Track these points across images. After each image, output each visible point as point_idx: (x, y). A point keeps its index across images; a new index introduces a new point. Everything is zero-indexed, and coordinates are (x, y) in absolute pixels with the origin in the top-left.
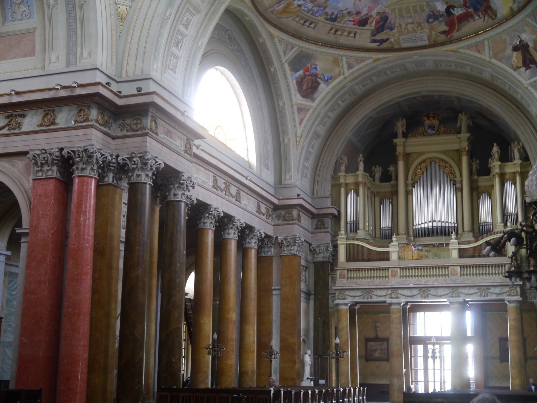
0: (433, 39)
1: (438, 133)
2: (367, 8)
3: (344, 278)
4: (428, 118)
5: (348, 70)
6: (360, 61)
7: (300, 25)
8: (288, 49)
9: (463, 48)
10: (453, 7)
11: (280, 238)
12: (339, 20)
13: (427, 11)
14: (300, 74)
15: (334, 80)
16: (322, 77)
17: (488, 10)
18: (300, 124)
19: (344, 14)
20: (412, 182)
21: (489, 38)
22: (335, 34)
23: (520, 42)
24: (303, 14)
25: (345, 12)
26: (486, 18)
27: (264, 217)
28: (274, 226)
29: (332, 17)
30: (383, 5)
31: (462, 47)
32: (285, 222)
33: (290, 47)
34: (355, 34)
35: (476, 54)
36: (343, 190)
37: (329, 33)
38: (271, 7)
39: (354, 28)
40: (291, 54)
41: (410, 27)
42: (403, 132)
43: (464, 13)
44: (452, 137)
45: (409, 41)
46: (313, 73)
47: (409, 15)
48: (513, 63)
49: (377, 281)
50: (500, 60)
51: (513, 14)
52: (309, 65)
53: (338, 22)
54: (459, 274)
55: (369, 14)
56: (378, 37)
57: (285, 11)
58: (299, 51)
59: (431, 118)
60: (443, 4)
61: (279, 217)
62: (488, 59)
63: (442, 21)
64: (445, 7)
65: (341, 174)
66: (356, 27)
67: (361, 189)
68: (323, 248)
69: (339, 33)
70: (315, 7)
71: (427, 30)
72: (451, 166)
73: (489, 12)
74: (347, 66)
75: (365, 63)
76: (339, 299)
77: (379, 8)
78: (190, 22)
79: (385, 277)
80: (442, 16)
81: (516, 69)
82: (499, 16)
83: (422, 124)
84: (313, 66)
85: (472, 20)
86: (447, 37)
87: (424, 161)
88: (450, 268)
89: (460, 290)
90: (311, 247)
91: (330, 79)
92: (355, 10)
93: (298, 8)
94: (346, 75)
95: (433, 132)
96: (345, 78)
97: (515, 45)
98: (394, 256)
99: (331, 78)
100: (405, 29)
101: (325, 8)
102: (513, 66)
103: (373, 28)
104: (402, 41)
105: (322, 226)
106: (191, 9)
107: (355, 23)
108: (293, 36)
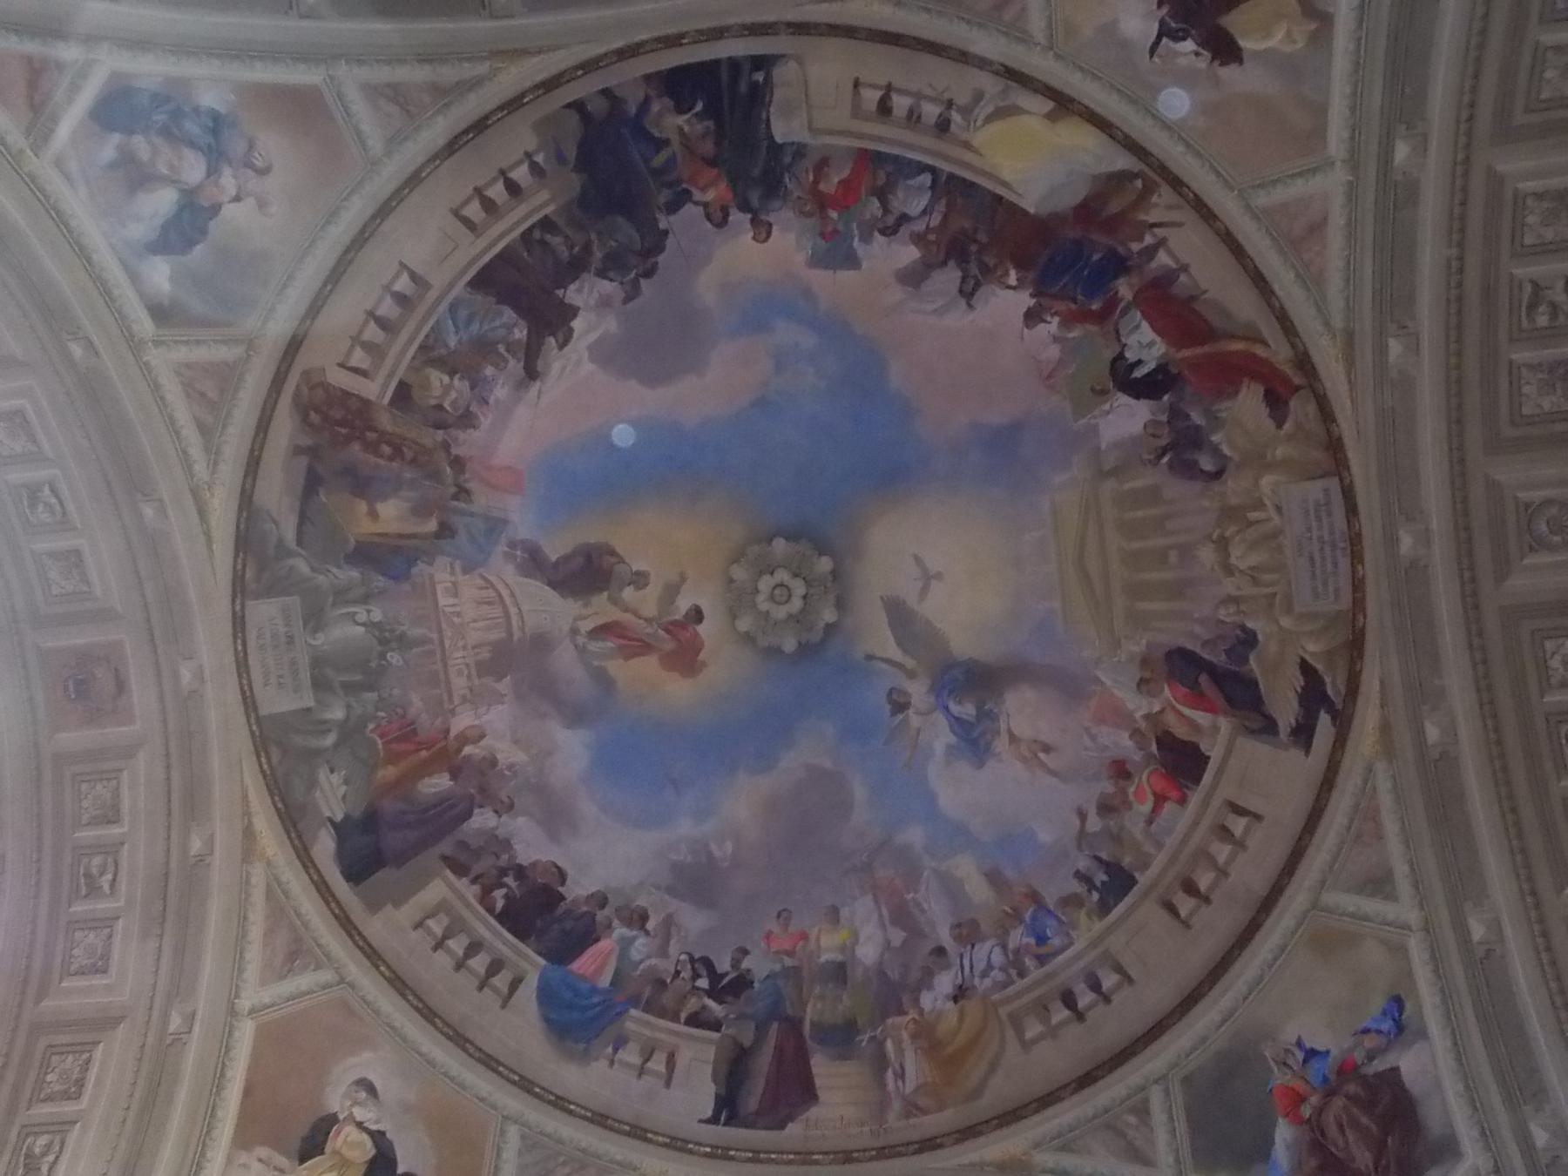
5: (1392, 897)
7: (1076, 1029)
8: (1131, 1133)
9: (1321, 308)
12: (1127, 861)
14: (1288, 1147)
16: (1370, 1042)
17: (1104, 214)
21: (1232, 189)
23: (1177, 37)
24: (1019, 995)
25: (1094, 824)
26: (1152, 218)
29: (1098, 884)
31: (1319, 310)
33: (1132, 1120)
34: (1240, 811)
37: (1186, 924)
39: (1205, 803)
41: (1241, 558)
43: (1146, 316)
45: (1329, 567)
46: (1325, 1079)
47: (1173, 557)
50: (1320, 111)
51: (1063, 105)
52: (1280, 1078)
53: (1145, 866)
55: (1143, 725)
58: (1176, 1088)
60: (1107, 407)
64: (1123, 399)
66: (1195, 798)
69: (1204, 881)
70: (1006, 933)
71: (1267, 481)
74: (1372, 895)
75: (1386, 801)
80: (1176, 413)
84: (1290, 1061)
85: (1183, 278)
86: (1298, 388)
91: (1401, 1009)
93: (972, 1006)
94: (1413, 917)
96: (1428, 928)
97: (1207, 54)
99: (1398, 1001)
100: (1255, 581)
101: (1035, 897)
102: (1314, 38)
103: (1225, 724)
107: (1174, 794)
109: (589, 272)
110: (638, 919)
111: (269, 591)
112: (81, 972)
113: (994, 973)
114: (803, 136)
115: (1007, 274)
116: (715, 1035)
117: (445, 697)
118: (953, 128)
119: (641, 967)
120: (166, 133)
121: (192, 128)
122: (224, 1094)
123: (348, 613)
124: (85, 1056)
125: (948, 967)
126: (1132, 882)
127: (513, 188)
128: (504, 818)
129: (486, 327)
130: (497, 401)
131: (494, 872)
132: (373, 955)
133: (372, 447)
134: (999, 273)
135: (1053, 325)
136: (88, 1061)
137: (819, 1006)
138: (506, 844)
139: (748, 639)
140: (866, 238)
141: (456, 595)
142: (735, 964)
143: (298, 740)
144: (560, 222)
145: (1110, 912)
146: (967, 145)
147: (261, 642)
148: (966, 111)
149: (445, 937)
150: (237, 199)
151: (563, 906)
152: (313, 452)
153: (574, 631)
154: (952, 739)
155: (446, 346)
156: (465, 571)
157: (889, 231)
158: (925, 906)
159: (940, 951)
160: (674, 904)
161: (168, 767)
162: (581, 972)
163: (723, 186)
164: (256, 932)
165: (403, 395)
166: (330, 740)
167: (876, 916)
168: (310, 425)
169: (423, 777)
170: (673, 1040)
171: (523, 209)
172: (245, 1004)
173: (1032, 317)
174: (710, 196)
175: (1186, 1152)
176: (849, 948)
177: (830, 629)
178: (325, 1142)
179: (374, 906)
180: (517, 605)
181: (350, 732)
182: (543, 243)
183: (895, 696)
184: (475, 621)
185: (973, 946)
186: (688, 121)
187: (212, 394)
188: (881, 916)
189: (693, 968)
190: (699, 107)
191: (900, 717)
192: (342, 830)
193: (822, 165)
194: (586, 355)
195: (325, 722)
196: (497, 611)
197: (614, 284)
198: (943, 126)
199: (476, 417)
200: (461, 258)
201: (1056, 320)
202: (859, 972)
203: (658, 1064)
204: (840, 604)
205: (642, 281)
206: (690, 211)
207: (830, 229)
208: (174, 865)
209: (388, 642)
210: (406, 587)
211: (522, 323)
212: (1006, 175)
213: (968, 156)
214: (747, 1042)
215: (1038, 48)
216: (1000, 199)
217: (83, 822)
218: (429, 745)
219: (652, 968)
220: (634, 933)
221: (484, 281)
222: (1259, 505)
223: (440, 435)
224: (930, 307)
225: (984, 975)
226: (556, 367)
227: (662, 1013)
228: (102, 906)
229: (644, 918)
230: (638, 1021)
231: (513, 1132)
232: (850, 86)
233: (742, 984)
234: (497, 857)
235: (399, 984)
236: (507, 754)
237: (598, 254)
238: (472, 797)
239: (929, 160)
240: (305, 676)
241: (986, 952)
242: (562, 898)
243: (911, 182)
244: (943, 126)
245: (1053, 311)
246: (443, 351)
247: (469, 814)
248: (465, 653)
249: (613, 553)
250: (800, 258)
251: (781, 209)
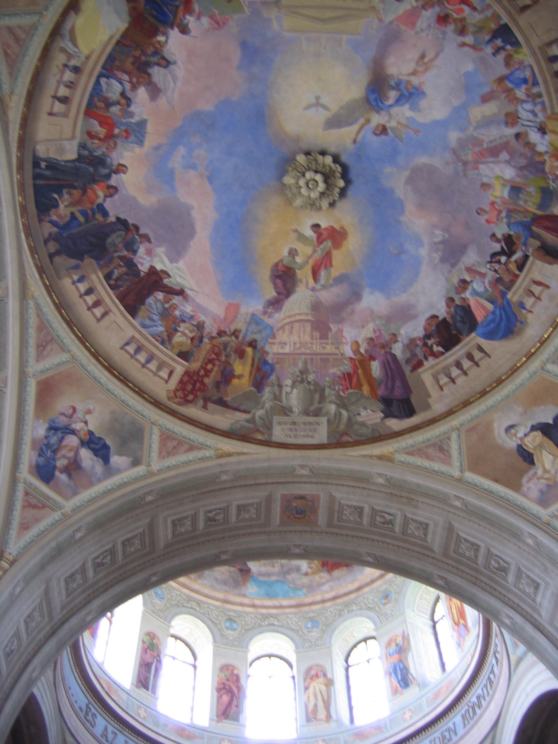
12: (493, 26)
19: (474, 33)
24: (551, 100)
25: (469, 39)
30: (380, 20)
53: (499, 17)
92: (444, 33)
93: (551, 125)
101: (501, 80)
109: (133, 258)
110: (464, 284)
111: (269, 428)
112: (425, 535)
113: (536, 111)
114: (74, 145)
115: (159, 42)
116: (531, 259)
117: (334, 357)
118: (78, 64)
119: (487, 287)
120: (55, 452)
121: (54, 440)
122: (494, 490)
123: (286, 396)
124: (462, 540)
125: (526, 134)
126: (506, 25)
127: (89, 291)
128: (399, 339)
129: (156, 312)
130: (193, 311)
131: (424, 349)
132: (450, 413)
133: (207, 373)
134: (158, 46)
135: (190, 20)
136: (465, 539)
137: (530, 204)
138: (412, 341)
139: (332, 205)
140: (131, 115)
141: (285, 344)
142: (498, 241)
143: (342, 427)
144: (107, 270)
145: (519, 42)
146: (88, 58)
147: (293, 436)
148: (70, 56)
149: (451, 378)
150: (86, 423)
151: (449, 319)
152: (206, 400)
153: (313, 289)
154: (407, 106)
155: (162, 332)
156: (274, 337)
157: (129, 101)
158: (492, 138)
160: (461, 266)
161: (343, 485)
162: (482, 317)
163: (96, 187)
164: (426, 463)
165: (184, 355)
166: (344, 413)
167: (491, 165)
168: (194, 400)
169: (371, 374)
170: (528, 279)
171: (100, 288)
172: (456, 473)
173: (184, 30)
174: (101, 194)
177: (336, 159)
178: (528, 452)
179: (428, 407)
180: (295, 315)
181: (342, 404)
182: (116, 280)
183: (378, 132)
184: (300, 337)
185: (519, 118)
186: (62, 202)
187: (175, 443)
188: (492, 162)
189: (496, 262)
190: (55, 196)
191: (389, 131)
192: (388, 414)
193: (90, 135)
194: (175, 264)
195: (335, 414)
196: (296, 325)
197: (141, 247)
198: (76, 70)
199: (199, 322)
200: (120, 320)
201: (188, 17)
202: (518, 180)
203: (536, 289)
204: (323, 153)
205: (142, 231)
206: (108, 205)
207: (124, 134)
208: (387, 491)
209: (303, 379)
210: (277, 366)
211: (156, 294)
212: (105, 38)
213: (94, 58)
214: (538, 243)
215: (41, 20)
216: (118, 43)
217: (360, 521)
218: (355, 368)
219: (490, 283)
220: (470, 288)
221: (133, 310)
223: (206, 340)
224: (172, 85)
225: (535, 115)
226: (179, 280)
227: (513, 282)
228: (398, 521)
229: (464, 282)
230: (515, 293)
231: (550, 367)
232: (52, 118)
233: (509, 240)
234: (418, 346)
235: (466, 404)
236: (368, 331)
237: (125, 253)
238: (386, 352)
239: (93, 80)
240: (312, 419)
242: (444, 320)
243: (104, 90)
244: (76, 70)
245: (183, 19)
246: (165, 333)
247: (394, 356)
248: (315, 344)
249: (277, 265)
250: (137, 150)
251: (111, 159)
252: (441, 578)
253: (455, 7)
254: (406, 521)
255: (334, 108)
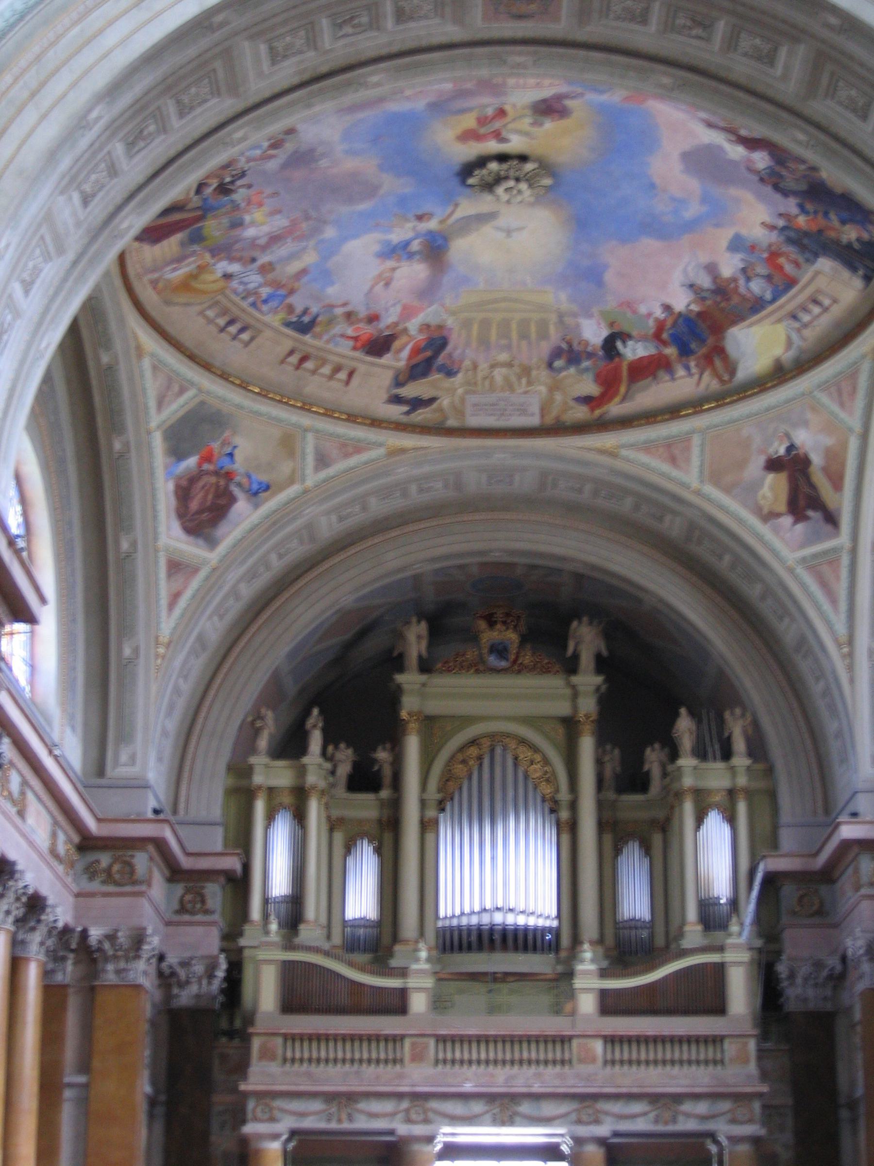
0: (554, 413)
1: (516, 667)
2: (398, 309)
3: (273, 1058)
4: (491, 624)
5: (317, 469)
6: (351, 450)
7: (213, 329)
10: (625, 337)
11: (95, 933)
12: (317, 329)
13: (555, 336)
15: (274, 494)
16: (244, 481)
18: (172, 605)
20: (439, 796)
22: (298, 367)
24: (231, 301)
25: (339, 311)
26: (707, 376)
27: (60, 869)
28: (78, 895)
30: (443, 305)
32: (111, 888)
34: (351, 374)
35: (665, 467)
36: (260, 807)
37: (283, 362)
38: (154, 271)
39: (353, 359)
40: (176, 408)
41: (499, 374)
42: (420, 657)
43: (650, 357)
44: (555, 682)
46: (222, 468)
47: (504, 342)
48: (762, 502)
49: (370, 1071)
50: (727, 490)
52: (216, 446)
54: (600, 1060)
55: (401, 327)
56: (410, 391)
57: (186, 285)
58: (197, 400)
59: (498, 626)
61: (91, 872)
62: (695, 484)
63: (587, 370)
64: (605, 333)
65: (259, 760)
66: (358, 354)
67: (314, 809)
68: (199, 968)
69: (309, 365)
71: (543, 389)
72: (546, 761)
73: (718, 363)
75: (364, 457)
76: (256, 1119)
77: (429, 314)
78: (38, 276)
79: (395, 1061)
80: (590, 355)
81: (769, 516)
82: (742, 374)
83: (474, 638)
85: (667, 377)
87: (473, 742)
88: (575, 1043)
89: (604, 1106)
90: (164, 965)
93: (221, 284)
94: (310, 483)
95: (504, 664)
98: (418, 1003)
99: (268, 488)
100: (485, 378)
101: (292, 292)
103: (402, 364)
104: (469, 410)
105: (198, 906)
106: (48, 239)
107: (359, 344)
108: (192, 357)
135: (659, 313)
146: (779, 321)
148: (799, 330)
157: (744, 270)
159: (254, 260)
173: (667, 308)
175: (170, 423)
176: (253, 223)
188: (276, 231)
193: (797, 265)
198: (794, 317)
206: (794, 210)
212: (755, 329)
222: (530, 383)
241: (254, 279)
250: (744, 232)
252: (222, 25)
253: (362, 332)
254: (312, 42)
255: (488, 230)
